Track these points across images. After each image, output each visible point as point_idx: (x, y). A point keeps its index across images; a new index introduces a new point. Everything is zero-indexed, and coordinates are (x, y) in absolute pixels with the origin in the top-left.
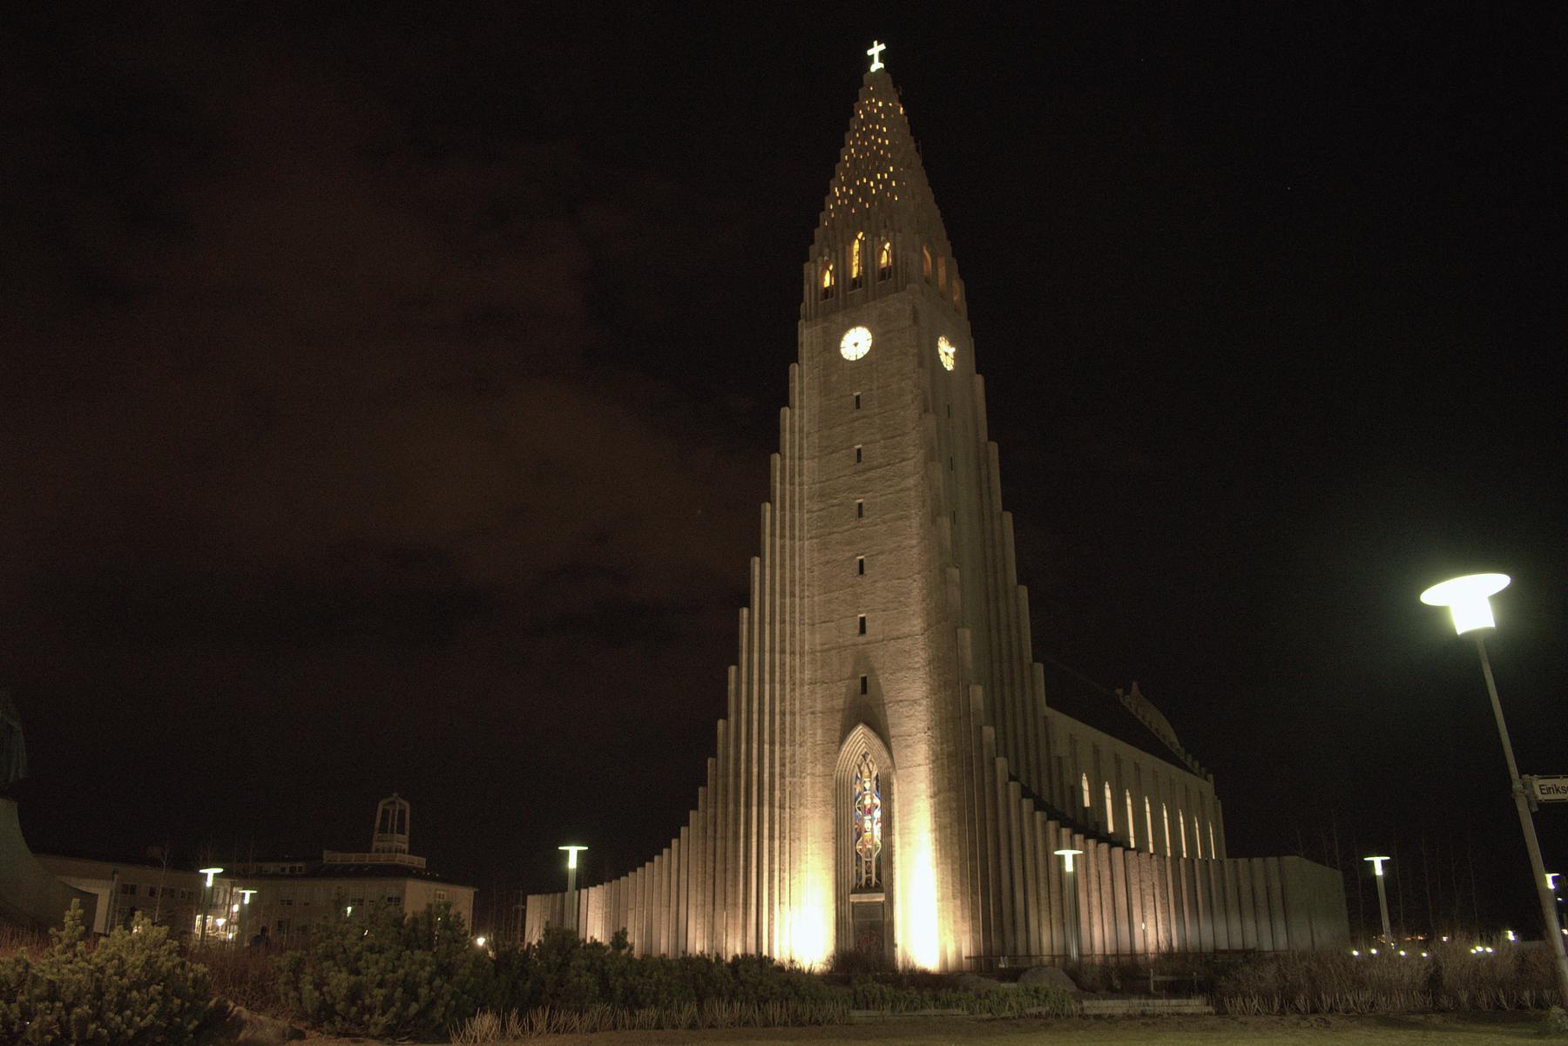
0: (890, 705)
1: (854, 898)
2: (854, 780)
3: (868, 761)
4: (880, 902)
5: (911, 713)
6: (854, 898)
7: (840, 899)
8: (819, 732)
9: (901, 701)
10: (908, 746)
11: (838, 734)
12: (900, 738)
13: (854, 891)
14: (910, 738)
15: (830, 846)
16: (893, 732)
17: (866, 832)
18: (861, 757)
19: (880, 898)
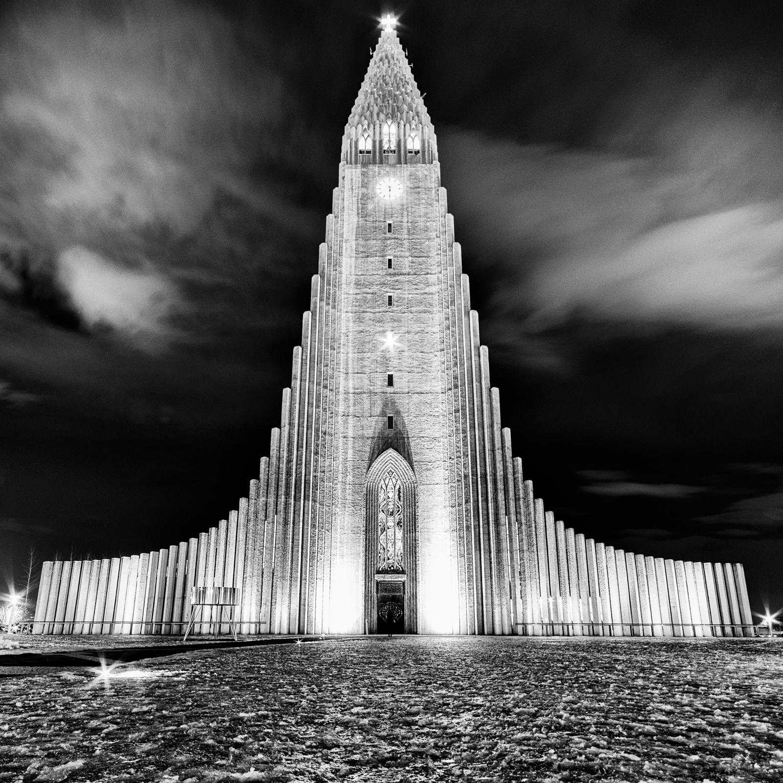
0: (413, 439)
1: (379, 578)
2: (379, 488)
3: (392, 477)
4: (401, 581)
5: (432, 446)
6: (379, 578)
7: (368, 577)
8: (350, 452)
9: (423, 437)
10: (428, 470)
11: (367, 455)
12: (421, 463)
13: (378, 572)
14: (431, 464)
15: (362, 537)
16: (415, 458)
17: (388, 528)
18: (386, 473)
19: (402, 578)
